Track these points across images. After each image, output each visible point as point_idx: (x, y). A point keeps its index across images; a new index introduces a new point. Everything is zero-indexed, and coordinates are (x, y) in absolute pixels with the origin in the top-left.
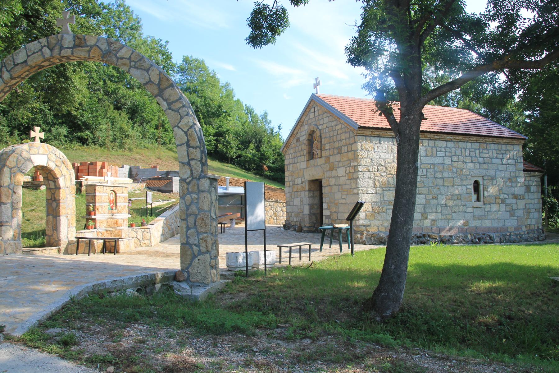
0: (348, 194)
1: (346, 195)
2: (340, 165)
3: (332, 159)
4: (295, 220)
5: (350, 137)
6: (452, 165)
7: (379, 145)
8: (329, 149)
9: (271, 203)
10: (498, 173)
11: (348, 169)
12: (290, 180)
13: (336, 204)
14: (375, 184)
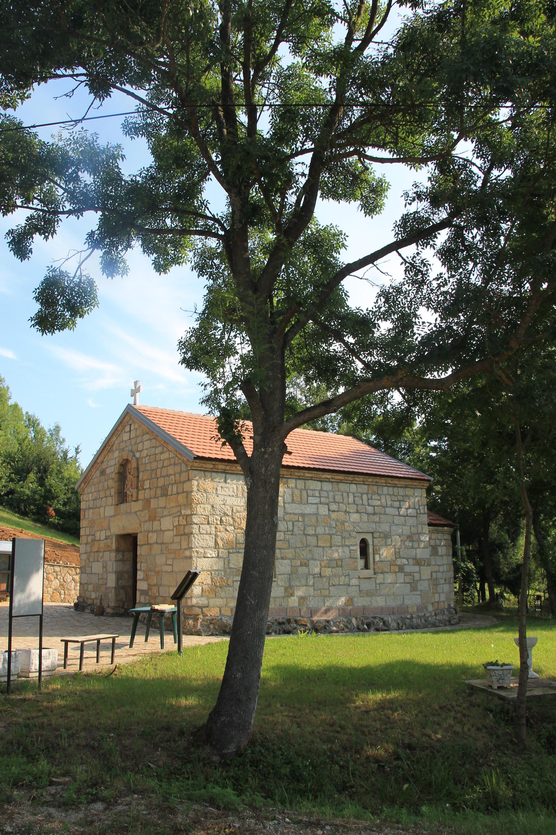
2: (166, 512)
3: (154, 504)
4: (93, 596)
5: (181, 472)
6: (329, 516)
7: (224, 485)
9: (58, 569)
10: (394, 528)
11: (177, 519)
12: (88, 533)
13: (158, 573)
14: (216, 543)
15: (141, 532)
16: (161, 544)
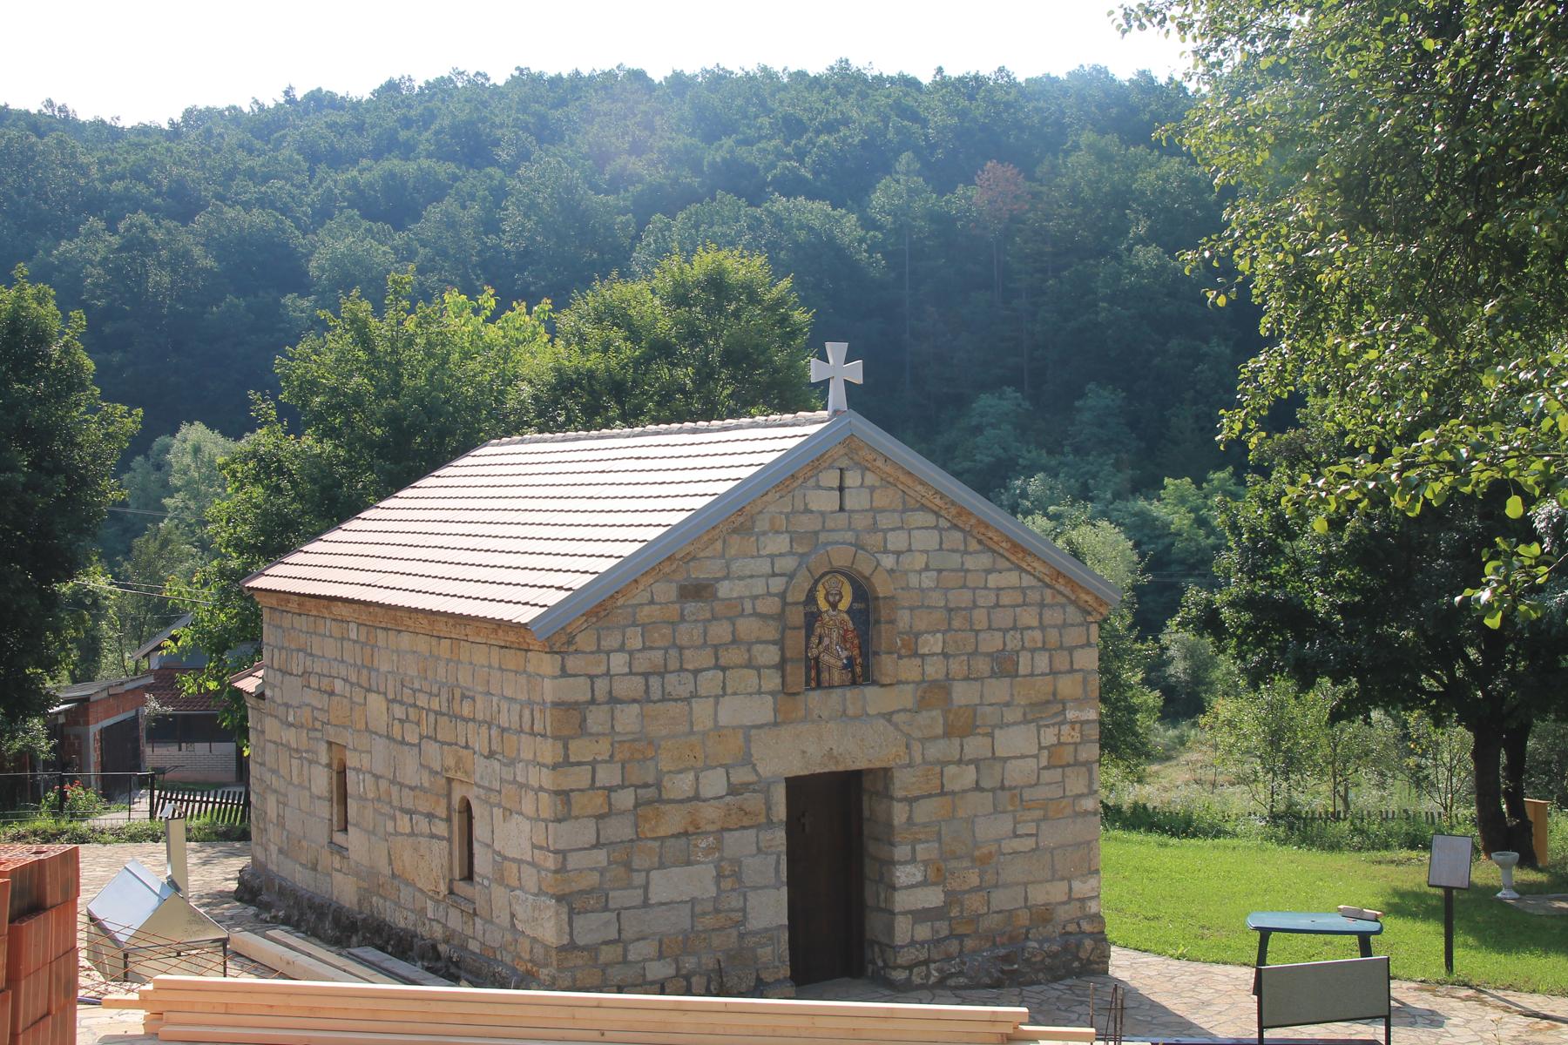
0: (1045, 818)
1: (1038, 822)
2: (1010, 716)
3: (963, 694)
5: (1065, 625)
8: (945, 655)
12: (617, 781)
13: (983, 861)
15: (910, 765)
16: (993, 790)
